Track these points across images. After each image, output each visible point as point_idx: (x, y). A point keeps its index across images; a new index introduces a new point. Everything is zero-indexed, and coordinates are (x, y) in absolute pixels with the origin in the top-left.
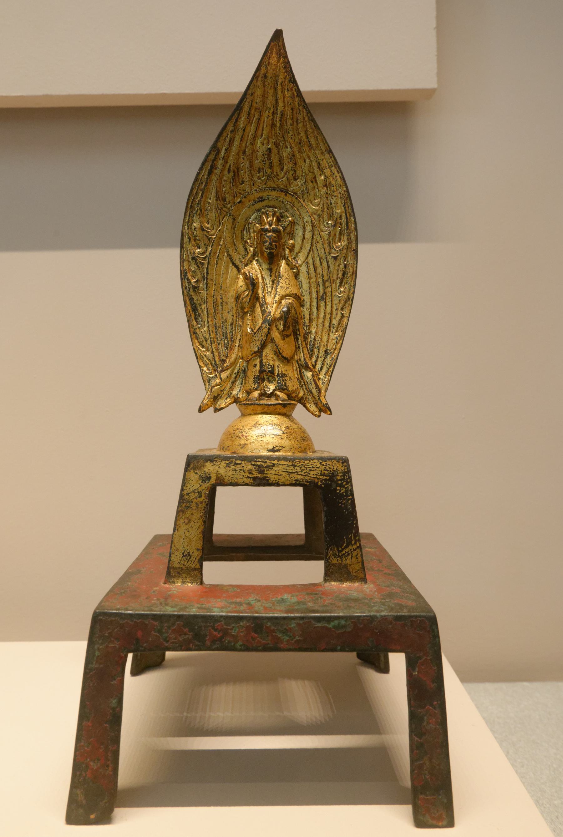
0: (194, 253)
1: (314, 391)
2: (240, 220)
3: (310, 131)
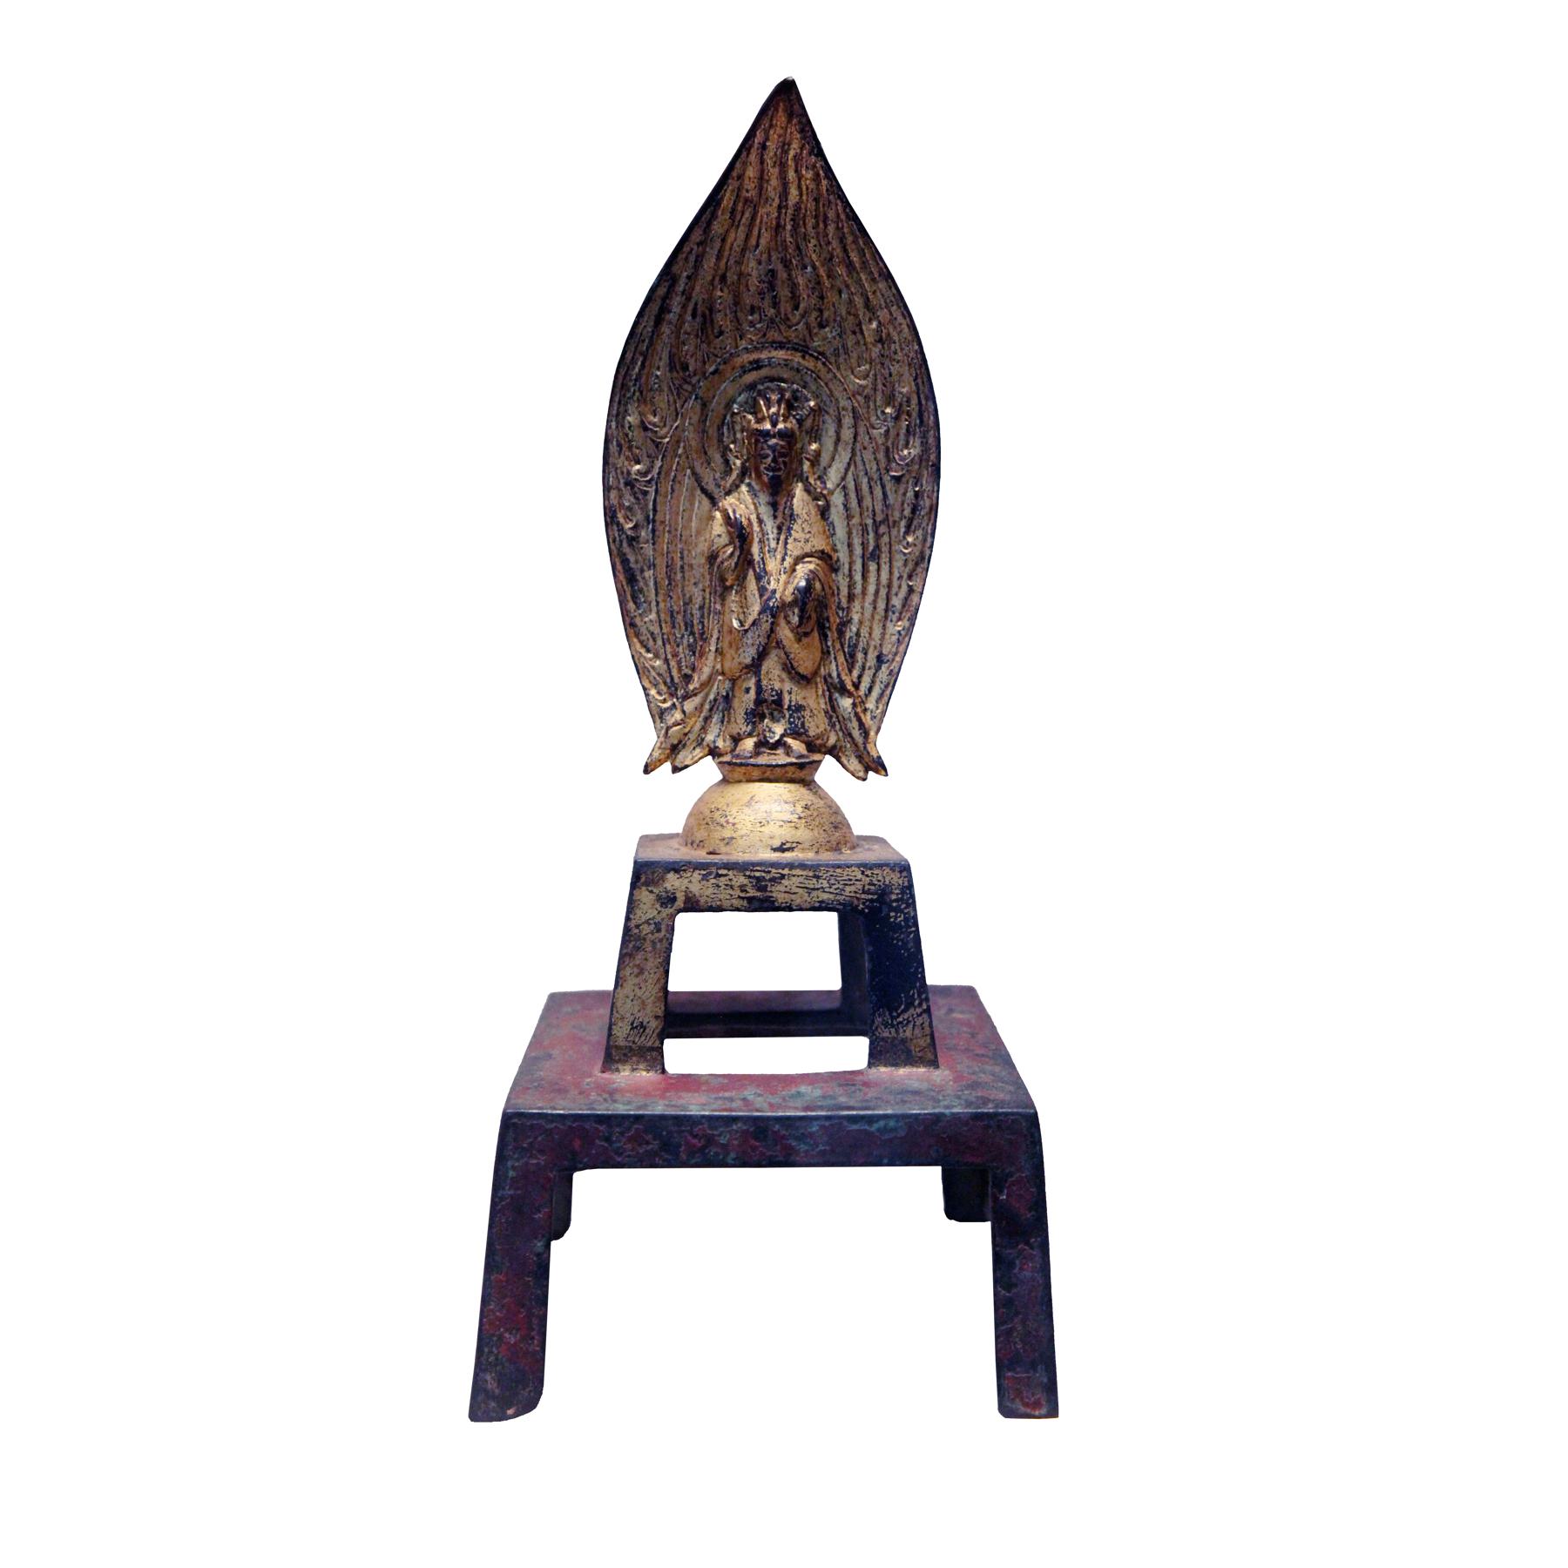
0: (629, 473)
1: (856, 733)
2: (716, 405)
3: (850, 239)
